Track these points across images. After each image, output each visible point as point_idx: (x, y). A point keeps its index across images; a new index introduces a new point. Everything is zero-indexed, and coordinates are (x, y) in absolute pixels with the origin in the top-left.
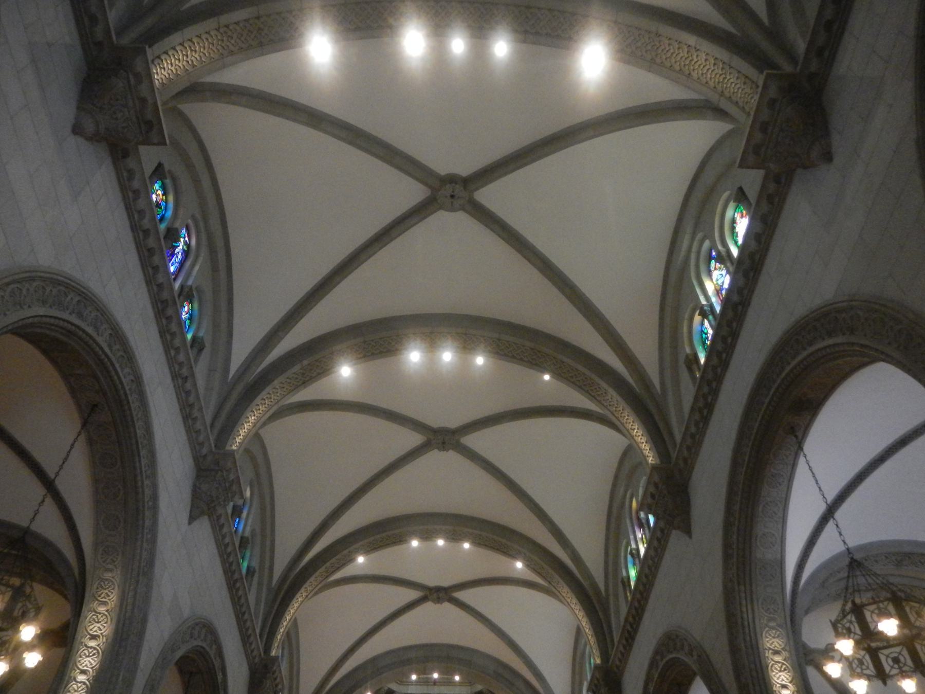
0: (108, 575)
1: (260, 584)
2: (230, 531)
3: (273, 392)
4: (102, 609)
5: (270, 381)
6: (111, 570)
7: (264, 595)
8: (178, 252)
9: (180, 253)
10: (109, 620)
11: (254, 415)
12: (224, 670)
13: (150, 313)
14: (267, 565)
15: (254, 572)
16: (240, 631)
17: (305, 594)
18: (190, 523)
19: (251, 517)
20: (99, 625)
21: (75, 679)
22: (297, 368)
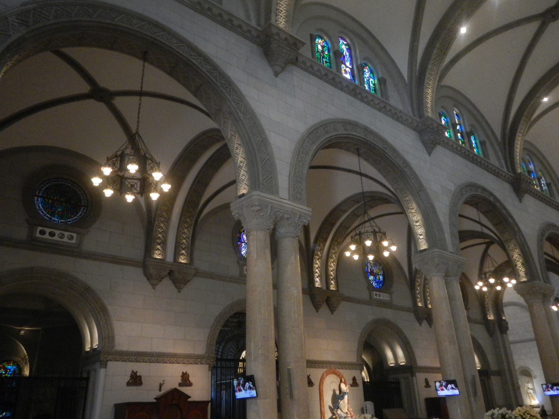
0: (407, 198)
1: (492, 145)
2: (454, 142)
3: (431, 71)
4: (413, 211)
5: (427, 67)
6: (407, 196)
7: (497, 148)
8: (346, 53)
9: (347, 52)
10: (418, 213)
11: (430, 89)
12: (491, 194)
13: (351, 98)
14: (490, 134)
15: (485, 142)
16: (491, 173)
17: (521, 135)
18: (430, 156)
19: (466, 121)
20: (416, 217)
21: (419, 238)
22: (435, 51)
